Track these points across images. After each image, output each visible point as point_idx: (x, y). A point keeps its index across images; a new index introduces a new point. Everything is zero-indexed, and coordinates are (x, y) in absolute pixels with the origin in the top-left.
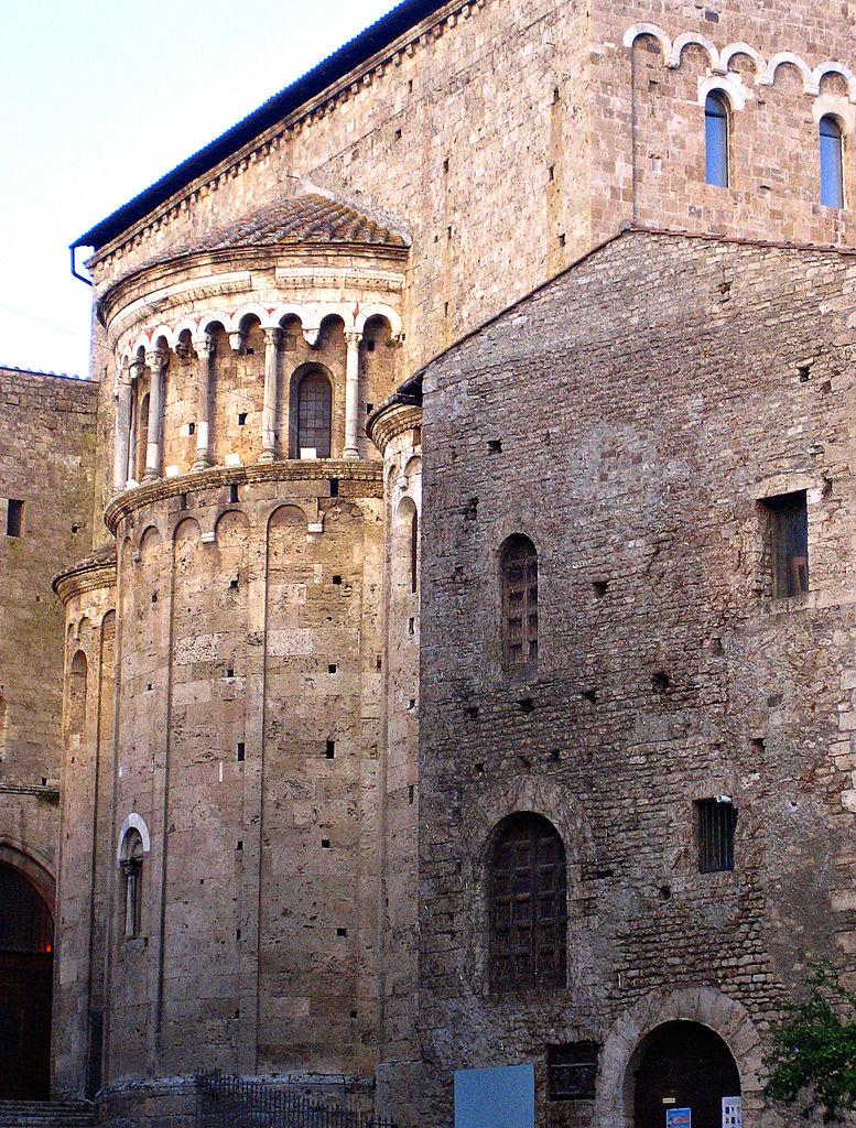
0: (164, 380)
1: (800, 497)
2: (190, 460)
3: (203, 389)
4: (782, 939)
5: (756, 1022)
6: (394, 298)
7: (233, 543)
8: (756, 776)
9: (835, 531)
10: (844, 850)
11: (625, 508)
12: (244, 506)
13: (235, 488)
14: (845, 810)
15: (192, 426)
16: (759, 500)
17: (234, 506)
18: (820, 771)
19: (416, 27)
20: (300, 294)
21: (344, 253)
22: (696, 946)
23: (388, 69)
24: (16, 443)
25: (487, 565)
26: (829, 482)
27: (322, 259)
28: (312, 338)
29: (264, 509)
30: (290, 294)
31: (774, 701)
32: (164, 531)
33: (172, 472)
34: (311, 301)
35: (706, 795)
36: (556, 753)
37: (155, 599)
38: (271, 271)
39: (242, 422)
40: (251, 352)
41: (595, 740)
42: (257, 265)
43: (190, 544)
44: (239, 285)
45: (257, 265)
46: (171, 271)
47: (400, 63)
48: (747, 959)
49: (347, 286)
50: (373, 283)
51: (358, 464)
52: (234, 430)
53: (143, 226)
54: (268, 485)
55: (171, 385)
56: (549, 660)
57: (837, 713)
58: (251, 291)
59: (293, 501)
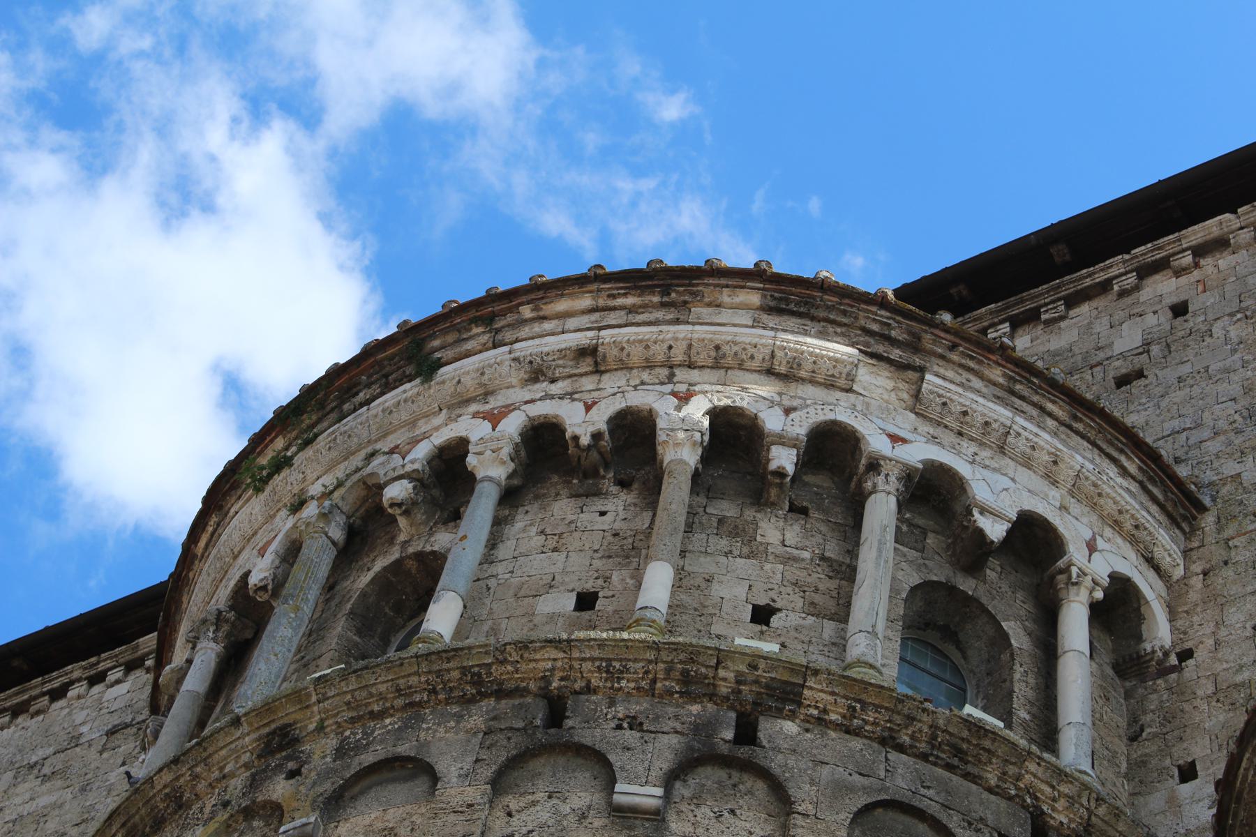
6: (1159, 584)
12: (775, 763)
17: (743, 752)
19: (1228, 215)
20: (969, 448)
21: (1079, 426)
23: (1085, 309)
27: (1035, 412)
28: (995, 531)
29: (840, 789)
30: (948, 438)
32: (450, 767)
34: (995, 470)
38: (911, 375)
40: (798, 510)
42: (880, 349)
44: (825, 366)
45: (880, 349)
46: (630, 300)
47: (1137, 288)
49: (1075, 490)
50: (1128, 525)
51: (1117, 813)
53: (76, 675)
54: (857, 744)
58: (849, 390)
59: (934, 809)
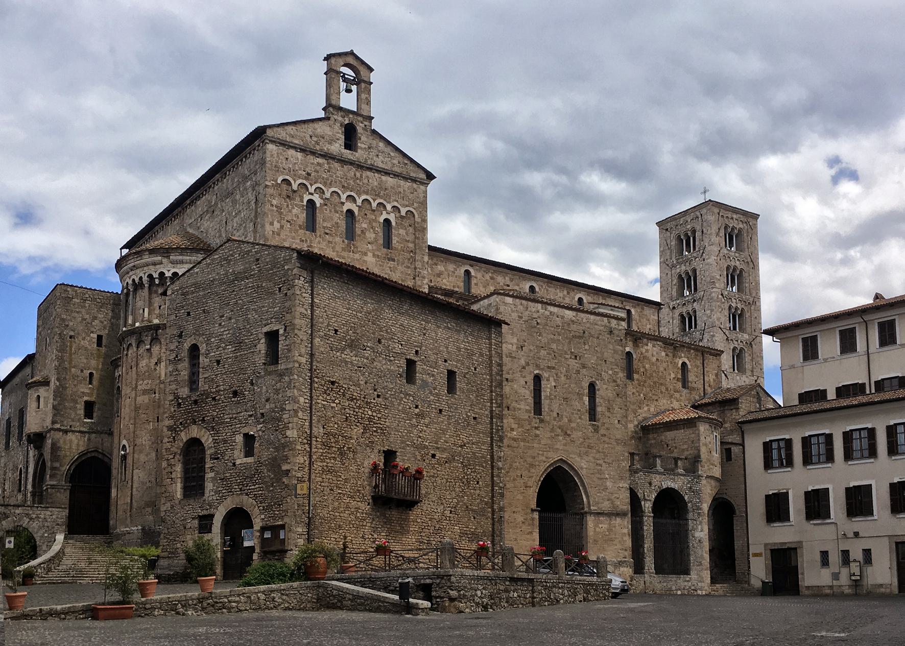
0: (134, 298)
1: (277, 331)
2: (143, 321)
3: (147, 297)
4: (267, 479)
5: (259, 507)
7: (156, 349)
8: (262, 425)
9: (287, 343)
10: (286, 450)
11: (226, 334)
12: (159, 337)
13: (157, 331)
14: (287, 437)
15: (144, 310)
16: (265, 333)
18: (280, 424)
22: (243, 482)
24: (100, 316)
25: (185, 354)
26: (286, 326)
31: (267, 400)
32: (134, 345)
33: (137, 324)
35: (247, 432)
36: (204, 418)
37: (131, 368)
39: (160, 309)
41: (215, 414)
43: (141, 350)
48: (257, 486)
52: (157, 311)
55: (138, 299)
56: (202, 386)
57: (286, 404)
